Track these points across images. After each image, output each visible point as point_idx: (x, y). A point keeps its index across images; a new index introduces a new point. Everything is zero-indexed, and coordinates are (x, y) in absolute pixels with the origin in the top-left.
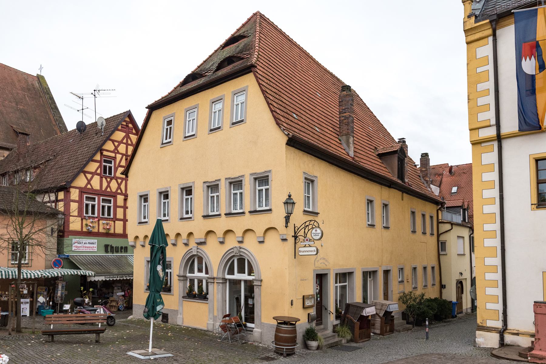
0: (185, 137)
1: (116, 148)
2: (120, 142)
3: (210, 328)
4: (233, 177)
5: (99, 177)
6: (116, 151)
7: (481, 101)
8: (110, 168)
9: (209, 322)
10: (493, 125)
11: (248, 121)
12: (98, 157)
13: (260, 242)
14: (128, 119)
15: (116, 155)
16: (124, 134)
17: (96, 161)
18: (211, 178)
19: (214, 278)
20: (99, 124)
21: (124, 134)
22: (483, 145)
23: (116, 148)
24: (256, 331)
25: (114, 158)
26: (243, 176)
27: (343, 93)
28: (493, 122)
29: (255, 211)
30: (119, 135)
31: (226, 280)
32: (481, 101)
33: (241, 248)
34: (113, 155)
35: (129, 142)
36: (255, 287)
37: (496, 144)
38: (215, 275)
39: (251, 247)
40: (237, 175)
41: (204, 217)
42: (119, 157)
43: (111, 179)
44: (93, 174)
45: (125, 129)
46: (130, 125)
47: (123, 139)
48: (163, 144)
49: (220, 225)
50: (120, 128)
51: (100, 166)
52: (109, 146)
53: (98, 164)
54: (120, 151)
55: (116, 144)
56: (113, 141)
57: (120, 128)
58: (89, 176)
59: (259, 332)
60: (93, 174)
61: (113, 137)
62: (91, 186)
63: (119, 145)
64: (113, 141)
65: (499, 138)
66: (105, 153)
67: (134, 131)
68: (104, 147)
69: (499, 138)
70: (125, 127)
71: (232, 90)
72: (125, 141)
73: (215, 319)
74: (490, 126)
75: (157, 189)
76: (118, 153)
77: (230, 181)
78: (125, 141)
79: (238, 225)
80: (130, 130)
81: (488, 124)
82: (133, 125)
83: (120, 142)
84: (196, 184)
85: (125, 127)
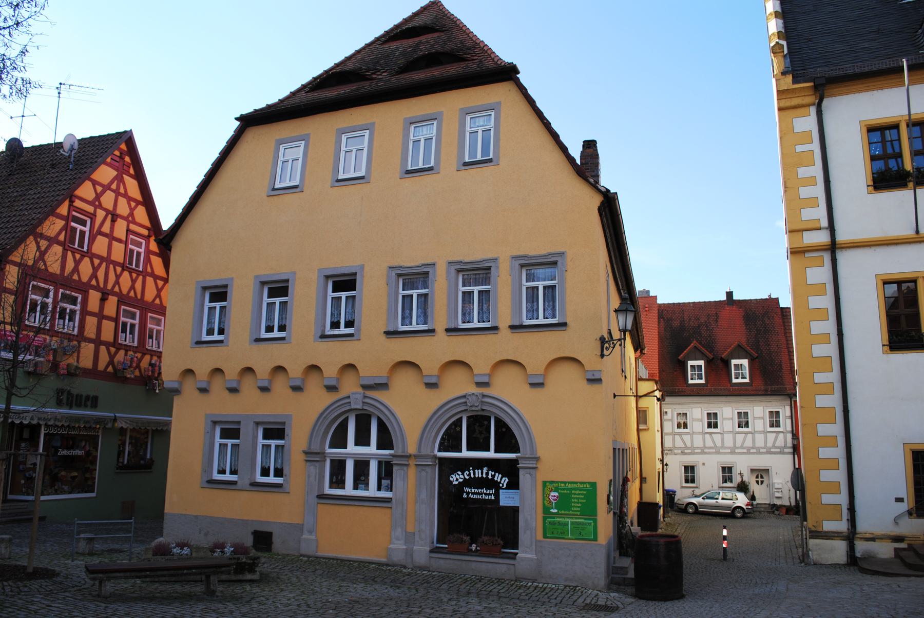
0: (338, 181)
1: (98, 196)
2: (107, 187)
3: (398, 557)
4: (467, 260)
5: (106, 240)
6: (96, 202)
7: (805, 192)
8: (82, 233)
9: (392, 546)
10: (824, 228)
11: (503, 161)
12: (64, 210)
13: (533, 385)
14: (123, 147)
15: (95, 211)
16: (115, 173)
17: (60, 217)
18: (411, 259)
19: (409, 457)
20: (67, 147)
21: (115, 173)
22: (807, 255)
23: (98, 196)
24: (523, 559)
25: (93, 216)
26: (495, 260)
27: (588, 150)
28: (825, 223)
29: (522, 327)
30: (105, 174)
31: (435, 457)
32: (805, 192)
33: (484, 396)
34: (90, 209)
35: (122, 190)
36: (521, 472)
37: (827, 257)
38: (412, 449)
39: (510, 393)
40: (478, 256)
41: (388, 333)
42: (101, 214)
43: (83, 256)
44: (52, 241)
45: (117, 164)
46: (127, 159)
47: (112, 182)
48: (274, 189)
49: (432, 352)
50: (109, 160)
51: (65, 227)
52: (86, 191)
53: (61, 223)
54: (105, 205)
55: (99, 189)
56: (95, 183)
57: (109, 160)
58: (44, 244)
59: (531, 559)
60: (52, 241)
61: (96, 176)
62: (45, 264)
63: (103, 192)
64: (95, 183)
65: (833, 247)
66: (78, 203)
67: (132, 171)
68: (80, 192)
69: (833, 247)
70: (118, 159)
71: (278, 138)
72: (114, 186)
73: (409, 538)
74: (820, 229)
75: (256, 277)
76: (100, 206)
77: (458, 267)
78: (114, 186)
79: (480, 352)
80: (125, 168)
81: (817, 226)
82: (131, 160)
83: (107, 187)
84: (367, 269)
85: (118, 159)
